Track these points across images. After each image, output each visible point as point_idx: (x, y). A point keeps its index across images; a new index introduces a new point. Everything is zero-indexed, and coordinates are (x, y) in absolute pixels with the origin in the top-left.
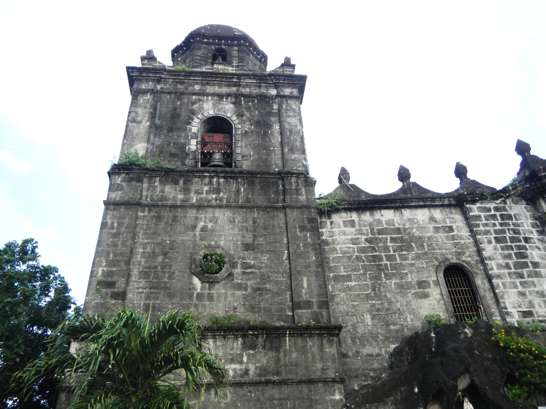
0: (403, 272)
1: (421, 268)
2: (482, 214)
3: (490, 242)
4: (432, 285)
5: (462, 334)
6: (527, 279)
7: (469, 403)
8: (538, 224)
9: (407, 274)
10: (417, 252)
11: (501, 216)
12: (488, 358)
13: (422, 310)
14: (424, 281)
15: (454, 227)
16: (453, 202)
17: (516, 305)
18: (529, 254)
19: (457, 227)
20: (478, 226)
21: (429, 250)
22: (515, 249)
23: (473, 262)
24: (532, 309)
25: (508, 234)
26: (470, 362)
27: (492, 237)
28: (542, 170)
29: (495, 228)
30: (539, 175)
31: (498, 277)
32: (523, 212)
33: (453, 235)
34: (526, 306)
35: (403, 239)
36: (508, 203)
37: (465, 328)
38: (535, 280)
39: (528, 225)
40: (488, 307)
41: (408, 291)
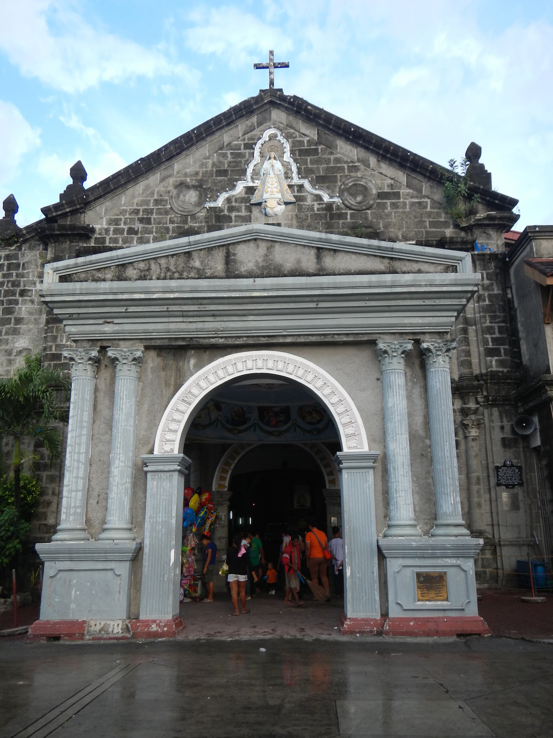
22: (5, 304)
25: (5, 287)
28: (53, 209)
36: (23, 249)
38: (10, 337)
39: (34, 276)
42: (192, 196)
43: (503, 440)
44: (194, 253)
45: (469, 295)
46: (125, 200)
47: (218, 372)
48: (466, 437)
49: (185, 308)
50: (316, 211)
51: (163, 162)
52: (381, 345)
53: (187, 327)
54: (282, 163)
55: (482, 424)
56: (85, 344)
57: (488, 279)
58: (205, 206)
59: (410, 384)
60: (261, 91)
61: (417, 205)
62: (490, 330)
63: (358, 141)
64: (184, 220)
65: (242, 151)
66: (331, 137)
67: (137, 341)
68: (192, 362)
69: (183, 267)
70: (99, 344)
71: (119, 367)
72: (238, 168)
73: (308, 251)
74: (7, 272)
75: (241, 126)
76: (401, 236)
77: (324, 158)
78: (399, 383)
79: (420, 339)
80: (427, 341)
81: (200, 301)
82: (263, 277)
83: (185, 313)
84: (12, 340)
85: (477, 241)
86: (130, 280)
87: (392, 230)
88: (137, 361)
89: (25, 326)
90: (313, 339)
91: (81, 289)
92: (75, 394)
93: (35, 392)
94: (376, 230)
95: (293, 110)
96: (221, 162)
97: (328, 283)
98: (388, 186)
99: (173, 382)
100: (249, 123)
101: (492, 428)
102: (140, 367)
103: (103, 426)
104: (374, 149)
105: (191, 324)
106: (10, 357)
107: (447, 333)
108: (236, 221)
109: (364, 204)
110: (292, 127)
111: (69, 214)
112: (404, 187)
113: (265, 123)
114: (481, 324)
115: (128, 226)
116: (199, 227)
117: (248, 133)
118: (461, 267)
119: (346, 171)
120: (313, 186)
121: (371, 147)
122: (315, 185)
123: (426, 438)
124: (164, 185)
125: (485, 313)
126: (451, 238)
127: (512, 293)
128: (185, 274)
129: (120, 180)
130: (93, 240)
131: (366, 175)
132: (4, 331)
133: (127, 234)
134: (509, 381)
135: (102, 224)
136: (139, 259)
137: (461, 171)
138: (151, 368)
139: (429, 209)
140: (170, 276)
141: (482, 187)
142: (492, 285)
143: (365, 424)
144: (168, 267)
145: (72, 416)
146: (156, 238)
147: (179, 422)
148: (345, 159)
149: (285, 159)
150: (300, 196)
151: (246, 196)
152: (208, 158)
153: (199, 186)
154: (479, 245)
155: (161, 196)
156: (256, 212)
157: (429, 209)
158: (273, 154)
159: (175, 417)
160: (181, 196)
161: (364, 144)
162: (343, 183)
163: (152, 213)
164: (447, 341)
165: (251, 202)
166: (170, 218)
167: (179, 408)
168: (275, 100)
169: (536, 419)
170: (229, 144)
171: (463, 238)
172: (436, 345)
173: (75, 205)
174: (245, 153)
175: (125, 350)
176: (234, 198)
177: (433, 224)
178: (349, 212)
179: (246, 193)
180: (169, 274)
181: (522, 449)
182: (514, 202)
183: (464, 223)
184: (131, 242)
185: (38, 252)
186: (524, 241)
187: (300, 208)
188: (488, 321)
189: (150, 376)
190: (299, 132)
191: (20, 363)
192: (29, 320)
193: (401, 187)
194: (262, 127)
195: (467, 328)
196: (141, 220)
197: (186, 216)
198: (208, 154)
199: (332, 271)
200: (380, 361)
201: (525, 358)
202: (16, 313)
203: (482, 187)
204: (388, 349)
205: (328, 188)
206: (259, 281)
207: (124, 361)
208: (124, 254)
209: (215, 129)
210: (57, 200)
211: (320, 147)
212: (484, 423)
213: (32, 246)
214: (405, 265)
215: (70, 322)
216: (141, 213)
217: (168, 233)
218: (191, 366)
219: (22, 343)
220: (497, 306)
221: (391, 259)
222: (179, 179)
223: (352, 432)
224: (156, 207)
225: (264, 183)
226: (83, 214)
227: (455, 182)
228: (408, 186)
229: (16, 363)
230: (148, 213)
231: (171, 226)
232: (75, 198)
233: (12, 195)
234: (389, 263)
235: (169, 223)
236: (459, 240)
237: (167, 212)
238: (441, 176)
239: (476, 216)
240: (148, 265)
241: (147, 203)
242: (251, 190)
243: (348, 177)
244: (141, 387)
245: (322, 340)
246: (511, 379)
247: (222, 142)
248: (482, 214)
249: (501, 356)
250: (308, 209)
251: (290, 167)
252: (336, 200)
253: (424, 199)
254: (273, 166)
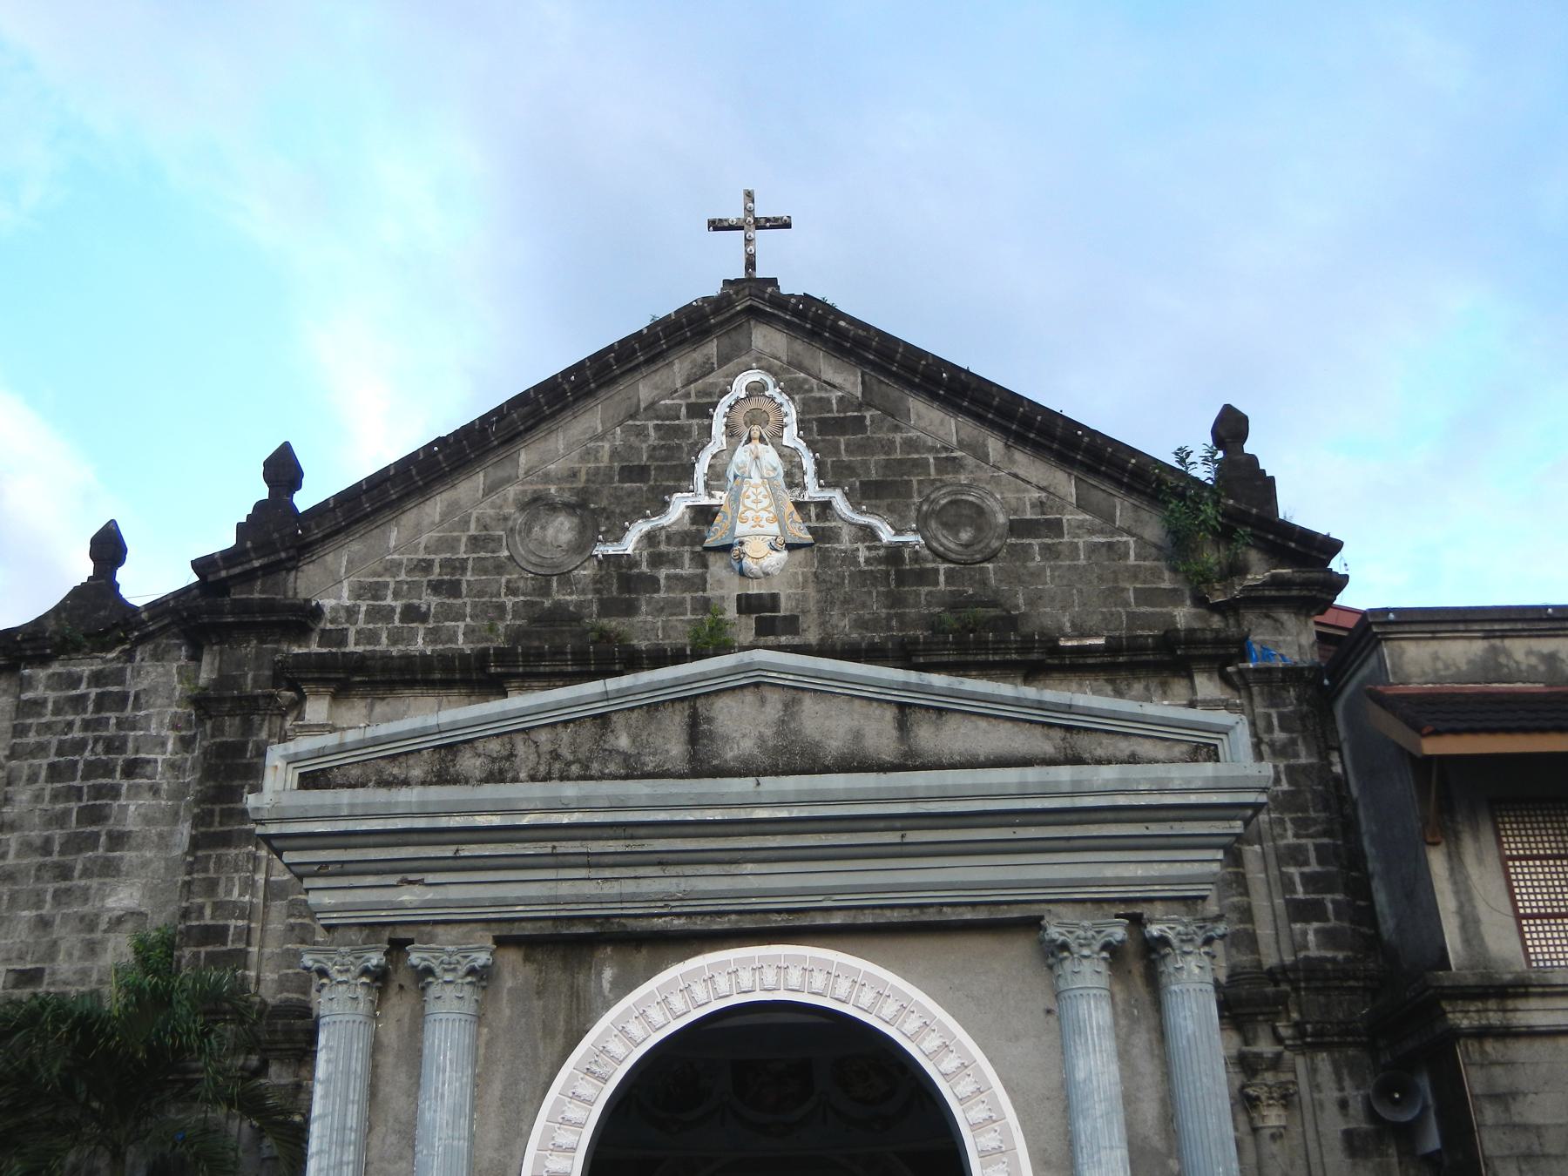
2: (51, 696)
3: (33, 779)
17: (14, 955)
22: (85, 797)
25: (87, 754)
27: (44, 762)
28: (221, 564)
29: (70, 736)
34: (37, 955)
36: (138, 658)
38: (94, 883)
39: (161, 724)
42: (561, 529)
43: (1348, 1135)
44: (614, 718)
45: (1249, 812)
46: (398, 539)
47: (671, 998)
48: (1255, 1130)
49: (595, 846)
50: (862, 565)
51: (495, 448)
52: (1054, 932)
53: (598, 891)
54: (778, 451)
55: (1292, 1095)
56: (353, 935)
57: (1283, 728)
58: (595, 553)
59: (1123, 1022)
60: (726, 282)
61: (1104, 550)
62: (1294, 855)
63: (959, 401)
64: (541, 588)
65: (683, 421)
66: (894, 391)
67: (479, 926)
68: (608, 974)
69: (591, 751)
70: (386, 934)
71: (434, 991)
72: (674, 463)
73: (877, 712)
74: (96, 716)
75: (681, 363)
76: (1068, 624)
77: (880, 440)
78: (1098, 1024)
79: (1141, 915)
80: (1160, 921)
81: (629, 831)
82: (777, 774)
83: (593, 860)
84: (99, 889)
85: (1251, 638)
86: (467, 782)
87: (1048, 610)
88: (482, 977)
89: (133, 854)
90: (895, 916)
91: (352, 805)
92: (328, 1061)
93: (181, 1036)
94: (1009, 612)
95: (804, 327)
96: (631, 447)
97: (928, 788)
98: (1033, 506)
99: (561, 1026)
100: (698, 356)
101: (1318, 1106)
102: (484, 988)
103: (392, 1139)
104: (997, 419)
105: (608, 884)
106: (93, 936)
107: (1204, 898)
108: (669, 589)
109: (977, 547)
110: (801, 368)
111: (260, 573)
112: (1070, 508)
113: (738, 356)
114: (1274, 839)
115: (404, 602)
116: (580, 605)
117: (696, 380)
118: (1227, 748)
119: (932, 470)
120: (856, 507)
121: (990, 416)
122: (860, 504)
123: (1169, 1155)
124: (492, 502)
125: (1281, 813)
126: (1191, 631)
127: (1342, 762)
128: (595, 767)
129: (388, 491)
130: (315, 637)
131: (980, 480)
132: (79, 867)
133: (401, 621)
134: (1352, 983)
135: (340, 598)
136: (489, 733)
137: (1202, 473)
138: (510, 990)
139: (1132, 560)
140: (561, 771)
141: (1254, 511)
142: (1293, 742)
143: (1022, 1123)
144: (555, 750)
145: (322, 1116)
146: (473, 631)
147: (582, 1125)
148: (930, 442)
149: (785, 443)
150: (823, 529)
151: (695, 527)
152: (601, 437)
153: (579, 506)
154: (1256, 647)
155: (485, 527)
156: (717, 566)
157: (1132, 560)
158: (756, 431)
159: (569, 1115)
160: (536, 529)
161: (974, 408)
162: (927, 499)
163: (464, 570)
164: (1204, 920)
165: (705, 545)
166: (509, 581)
167: (579, 1091)
168: (761, 306)
169: (1424, 1083)
170: (651, 406)
171: (1217, 631)
172: (1180, 928)
173: (277, 552)
174: (691, 425)
175: (450, 948)
176: (663, 533)
177: (1144, 596)
178: (943, 567)
179: (694, 521)
180: (557, 766)
181: (1395, 1160)
182: (1334, 547)
183: (1218, 593)
184: (411, 639)
185: (175, 665)
186: (1362, 644)
187: (824, 558)
188: (1290, 833)
189: (507, 1012)
190: (820, 379)
191: (119, 949)
192: (144, 837)
193: (1064, 507)
194: (730, 367)
195: (1240, 851)
196: (436, 587)
197: (548, 578)
198: (600, 429)
199: (934, 759)
200: (1051, 967)
201: (1388, 925)
202: (112, 821)
203: (1254, 511)
204: (1070, 939)
205: (891, 509)
206: (769, 783)
207: (448, 977)
208: (454, 722)
209: (618, 372)
210: (228, 540)
211: (868, 415)
212: (1296, 1092)
213: (159, 651)
214: (1100, 744)
215: (320, 882)
216: (437, 570)
217: (502, 618)
218: (606, 985)
219: (123, 897)
220: (1309, 796)
221: (1069, 728)
222: (530, 488)
223: (995, 1144)
224: (475, 556)
225: (736, 499)
226: (293, 573)
227: (1190, 497)
228: (1081, 505)
229: (106, 950)
230: (454, 568)
231: (509, 601)
232: (276, 536)
233: (113, 522)
234: (1064, 739)
235: (506, 595)
236: (1209, 635)
237: (499, 568)
238: (1159, 485)
239: (1245, 579)
240: (508, 747)
241: (452, 545)
242: (704, 515)
243: (938, 484)
244: (483, 1039)
245: (915, 919)
246: (1357, 979)
247: (635, 400)
248: (1259, 572)
249: (1328, 920)
250: (843, 560)
251: (797, 459)
252: (910, 538)
253: (1122, 536)
254: (757, 457)
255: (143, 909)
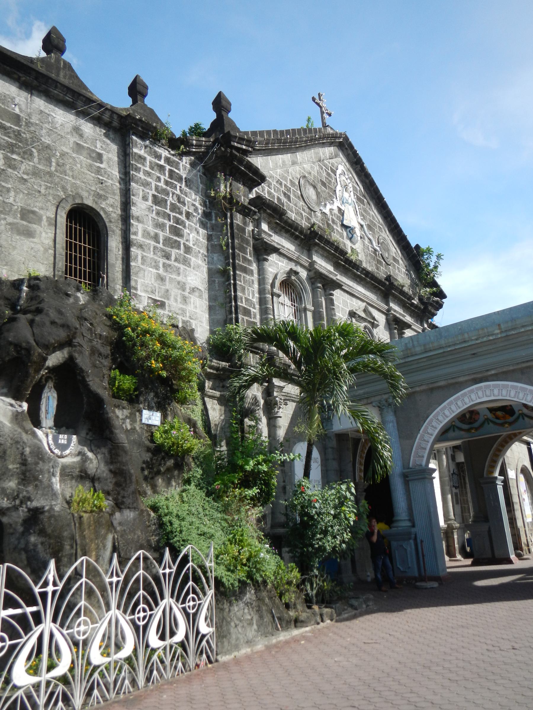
0: (3, 184)
1: (35, 191)
2: (149, 158)
4: (44, 222)
5: (72, 297)
6: (172, 263)
7: (53, 389)
8: (208, 203)
9: (8, 190)
10: (37, 165)
11: (171, 171)
12: (101, 335)
13: (15, 252)
14: (33, 212)
15: (105, 157)
16: (115, 124)
17: (149, 289)
18: (185, 234)
19: (109, 159)
20: (138, 170)
21: (56, 171)
22: (172, 221)
23: (113, 215)
24: (165, 301)
25: (171, 198)
26: (78, 331)
30: (232, 143)
31: (141, 246)
32: (197, 180)
33: (99, 167)
34: (160, 294)
35: (20, 135)
37: (78, 289)
38: (182, 267)
40: (114, 280)
41: (2, 216)
196: (285, 194)
229: (191, 302)
255: (200, 288)
